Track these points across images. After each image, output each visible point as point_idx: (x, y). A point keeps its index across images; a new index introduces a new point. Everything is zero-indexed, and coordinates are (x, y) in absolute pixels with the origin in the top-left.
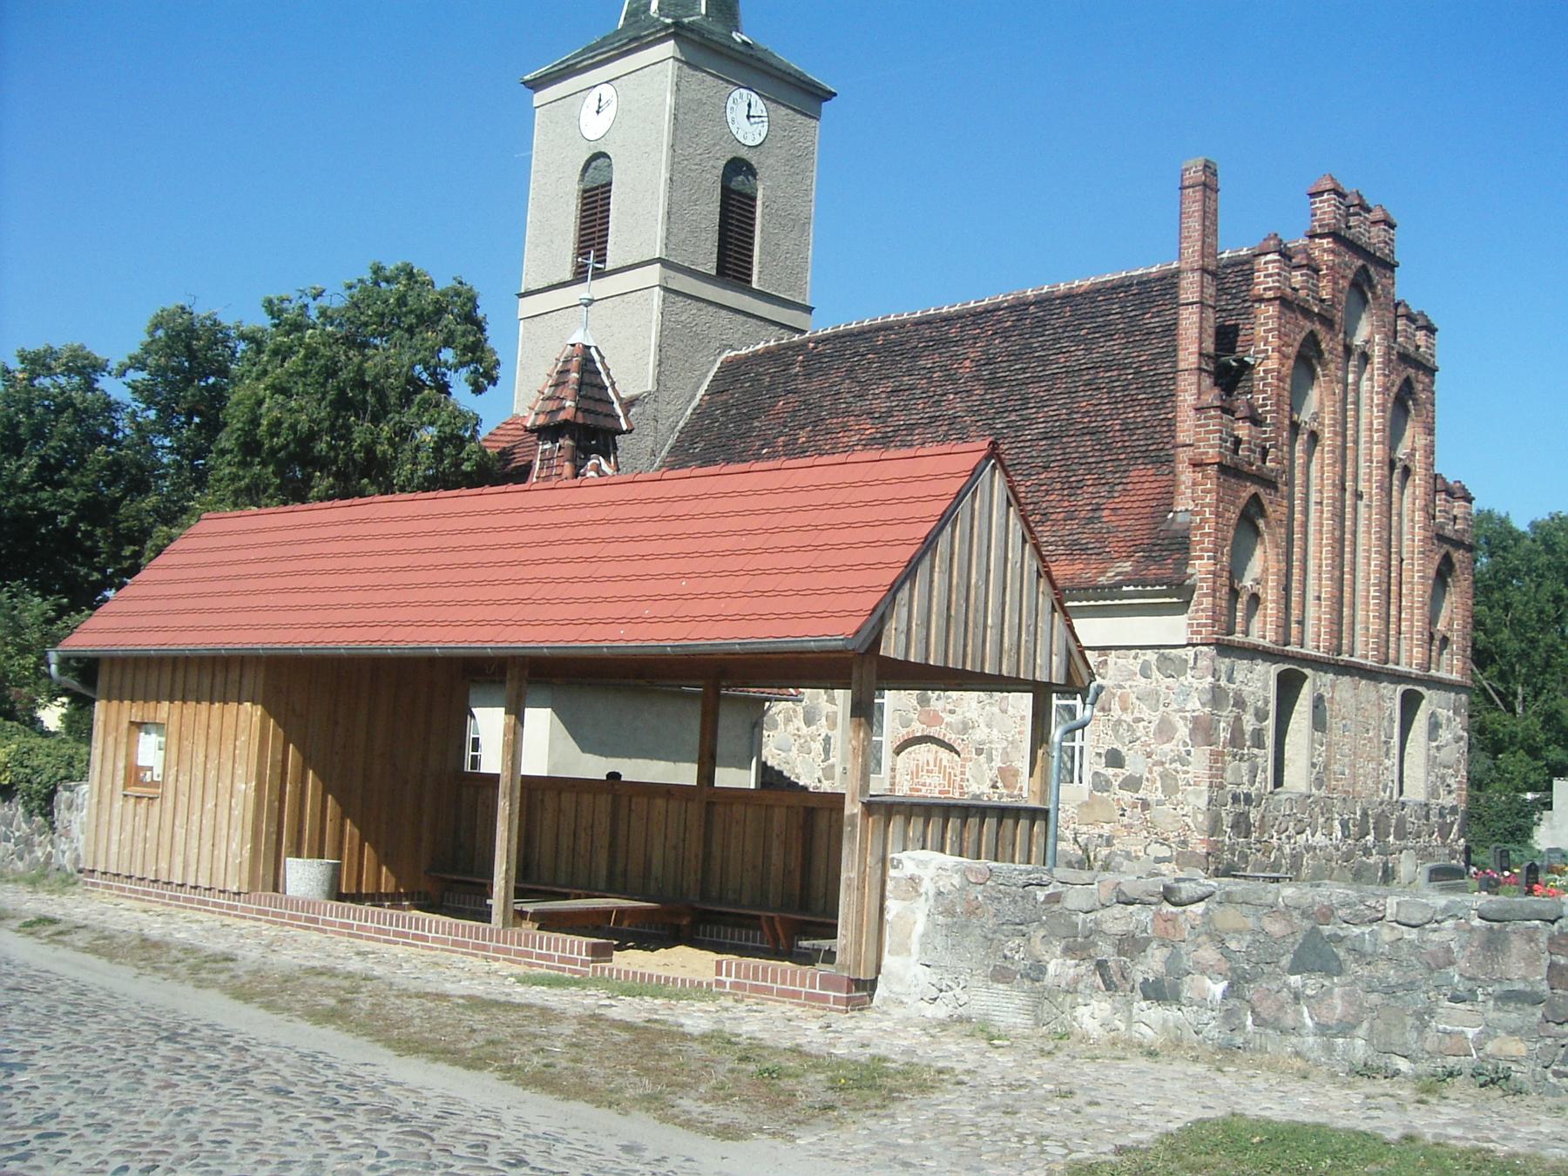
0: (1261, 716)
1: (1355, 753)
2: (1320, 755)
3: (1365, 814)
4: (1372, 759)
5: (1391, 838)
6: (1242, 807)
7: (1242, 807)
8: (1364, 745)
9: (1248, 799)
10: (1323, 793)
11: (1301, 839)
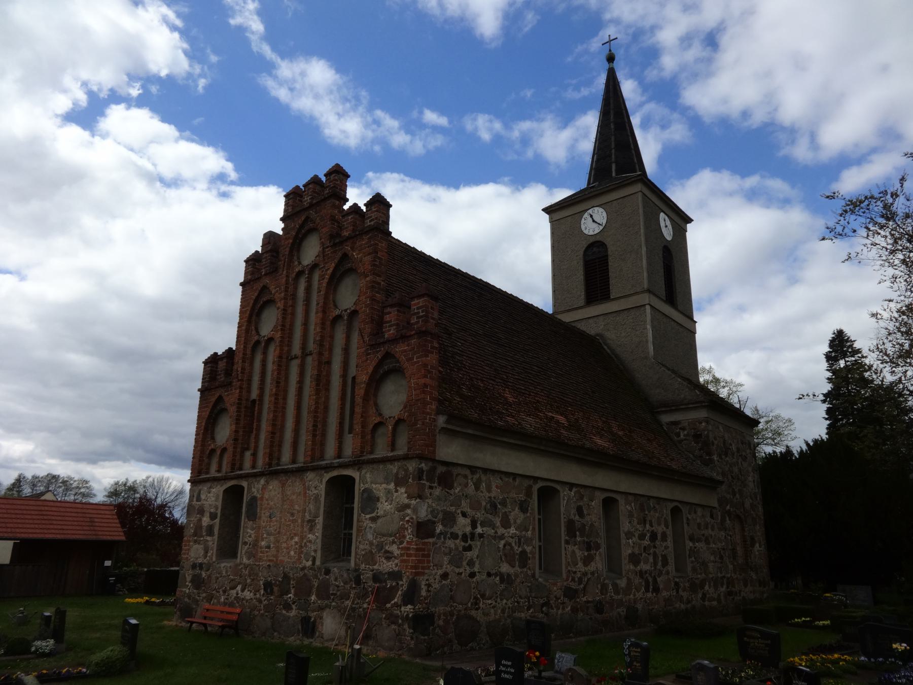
0: (213, 516)
1: (279, 533)
2: (250, 536)
3: (286, 577)
4: (296, 535)
5: (313, 598)
6: (197, 571)
7: (197, 571)
8: (287, 526)
9: (201, 566)
10: (251, 562)
11: (233, 592)
